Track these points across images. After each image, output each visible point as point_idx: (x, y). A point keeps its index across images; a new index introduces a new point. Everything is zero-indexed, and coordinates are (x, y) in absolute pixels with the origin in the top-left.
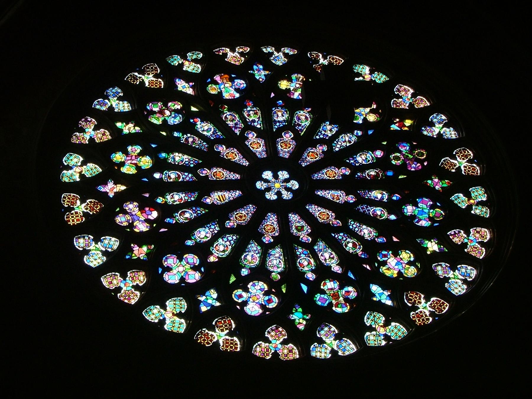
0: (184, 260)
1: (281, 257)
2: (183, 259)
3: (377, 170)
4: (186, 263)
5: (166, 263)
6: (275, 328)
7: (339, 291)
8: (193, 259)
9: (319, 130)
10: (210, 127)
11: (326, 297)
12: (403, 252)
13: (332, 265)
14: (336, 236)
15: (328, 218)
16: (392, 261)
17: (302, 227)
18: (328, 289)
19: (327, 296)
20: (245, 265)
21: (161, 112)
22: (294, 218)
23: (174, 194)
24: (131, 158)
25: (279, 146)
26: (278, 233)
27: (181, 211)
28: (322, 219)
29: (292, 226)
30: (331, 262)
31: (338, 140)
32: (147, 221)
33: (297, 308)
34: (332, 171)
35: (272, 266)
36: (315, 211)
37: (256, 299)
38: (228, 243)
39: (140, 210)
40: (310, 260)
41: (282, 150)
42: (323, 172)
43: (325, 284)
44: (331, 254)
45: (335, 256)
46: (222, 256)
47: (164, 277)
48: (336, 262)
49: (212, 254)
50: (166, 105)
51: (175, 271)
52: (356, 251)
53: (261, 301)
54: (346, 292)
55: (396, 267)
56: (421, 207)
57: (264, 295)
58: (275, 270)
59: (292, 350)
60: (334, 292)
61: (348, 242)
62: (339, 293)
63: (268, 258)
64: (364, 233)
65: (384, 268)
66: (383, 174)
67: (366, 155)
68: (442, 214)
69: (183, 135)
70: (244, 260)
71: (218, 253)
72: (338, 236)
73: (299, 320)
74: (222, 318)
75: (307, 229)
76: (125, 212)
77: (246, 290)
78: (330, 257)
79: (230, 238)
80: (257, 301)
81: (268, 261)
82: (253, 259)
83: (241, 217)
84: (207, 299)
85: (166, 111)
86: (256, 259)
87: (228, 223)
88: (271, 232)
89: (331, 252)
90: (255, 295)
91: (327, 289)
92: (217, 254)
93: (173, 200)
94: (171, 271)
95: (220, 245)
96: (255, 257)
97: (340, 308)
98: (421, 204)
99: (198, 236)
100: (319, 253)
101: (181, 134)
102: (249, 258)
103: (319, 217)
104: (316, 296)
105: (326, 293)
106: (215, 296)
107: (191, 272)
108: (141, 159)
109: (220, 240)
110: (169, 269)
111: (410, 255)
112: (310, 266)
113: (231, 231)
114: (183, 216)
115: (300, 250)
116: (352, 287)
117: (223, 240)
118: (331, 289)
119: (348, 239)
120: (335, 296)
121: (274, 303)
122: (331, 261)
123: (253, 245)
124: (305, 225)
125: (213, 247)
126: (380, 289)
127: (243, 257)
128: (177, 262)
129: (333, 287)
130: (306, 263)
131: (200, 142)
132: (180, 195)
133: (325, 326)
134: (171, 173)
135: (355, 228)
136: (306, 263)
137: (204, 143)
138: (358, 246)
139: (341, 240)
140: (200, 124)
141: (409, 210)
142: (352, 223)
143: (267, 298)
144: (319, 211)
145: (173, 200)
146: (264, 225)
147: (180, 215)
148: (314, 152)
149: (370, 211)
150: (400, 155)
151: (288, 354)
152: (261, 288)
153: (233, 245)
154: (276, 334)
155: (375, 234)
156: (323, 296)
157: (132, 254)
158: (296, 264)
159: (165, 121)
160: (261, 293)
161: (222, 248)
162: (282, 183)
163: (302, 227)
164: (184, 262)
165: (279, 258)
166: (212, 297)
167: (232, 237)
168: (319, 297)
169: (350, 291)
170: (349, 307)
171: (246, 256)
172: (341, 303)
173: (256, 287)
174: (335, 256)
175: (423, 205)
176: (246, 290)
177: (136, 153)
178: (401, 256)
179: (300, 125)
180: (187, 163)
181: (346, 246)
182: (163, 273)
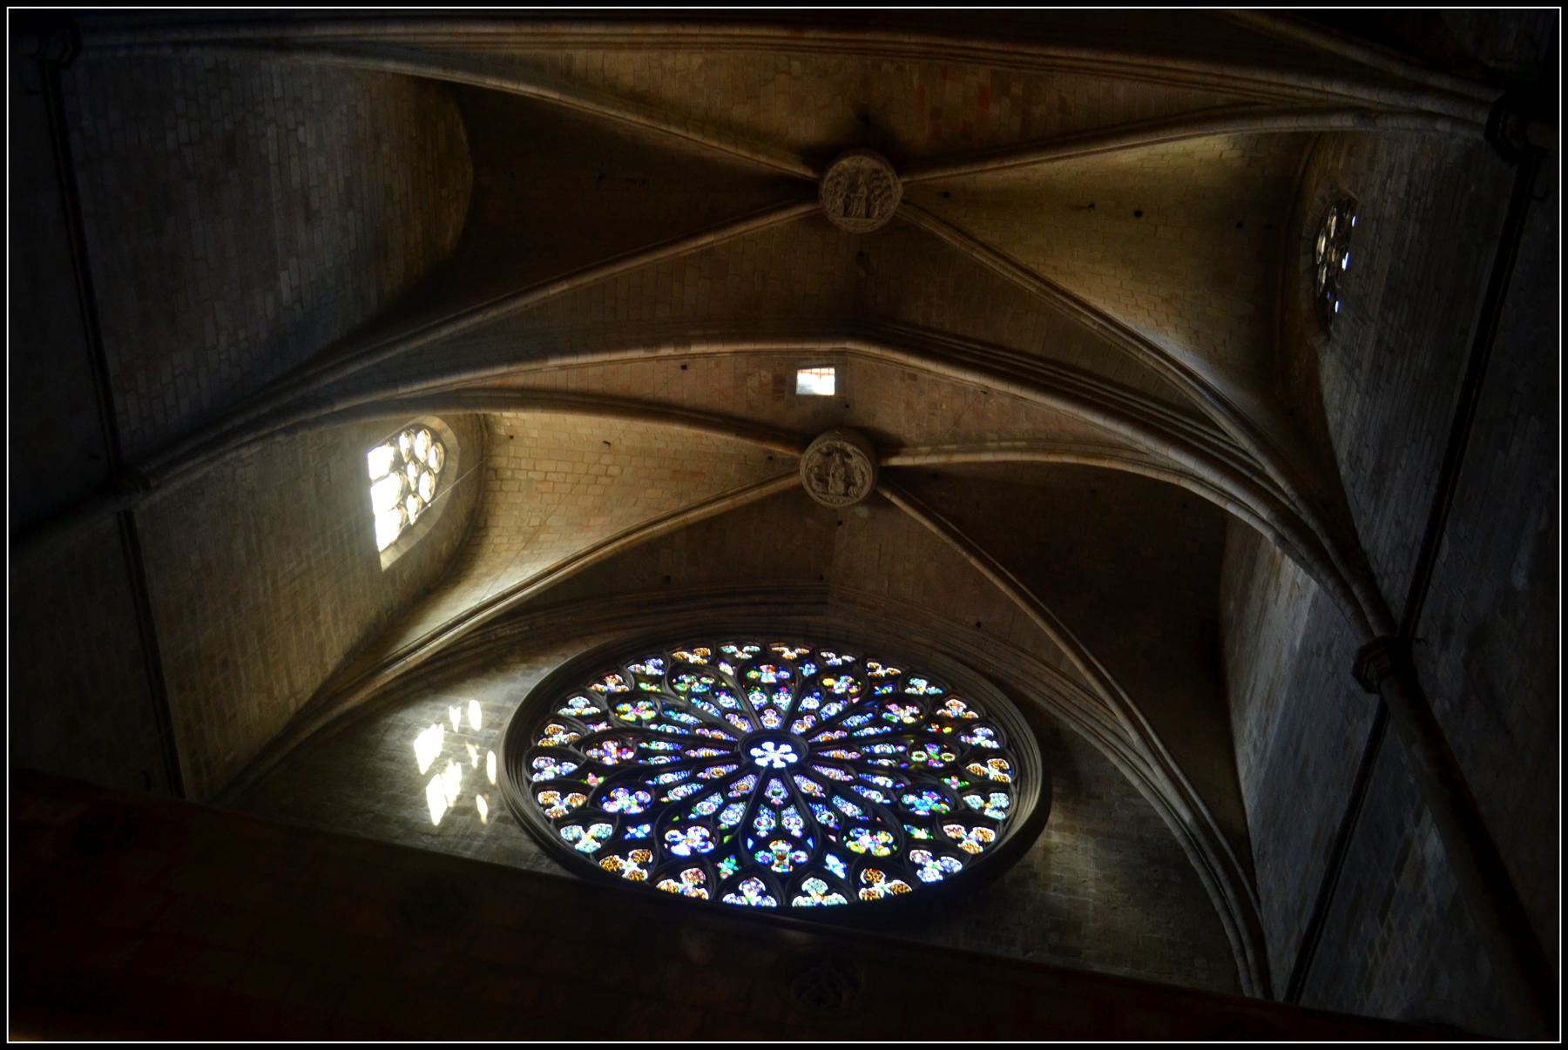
49: (667, 796)
53: (695, 845)
75: (784, 794)
110: (613, 800)
113: (701, 781)
136: (764, 822)
143: (703, 844)
156: (767, 854)
182: (606, 801)
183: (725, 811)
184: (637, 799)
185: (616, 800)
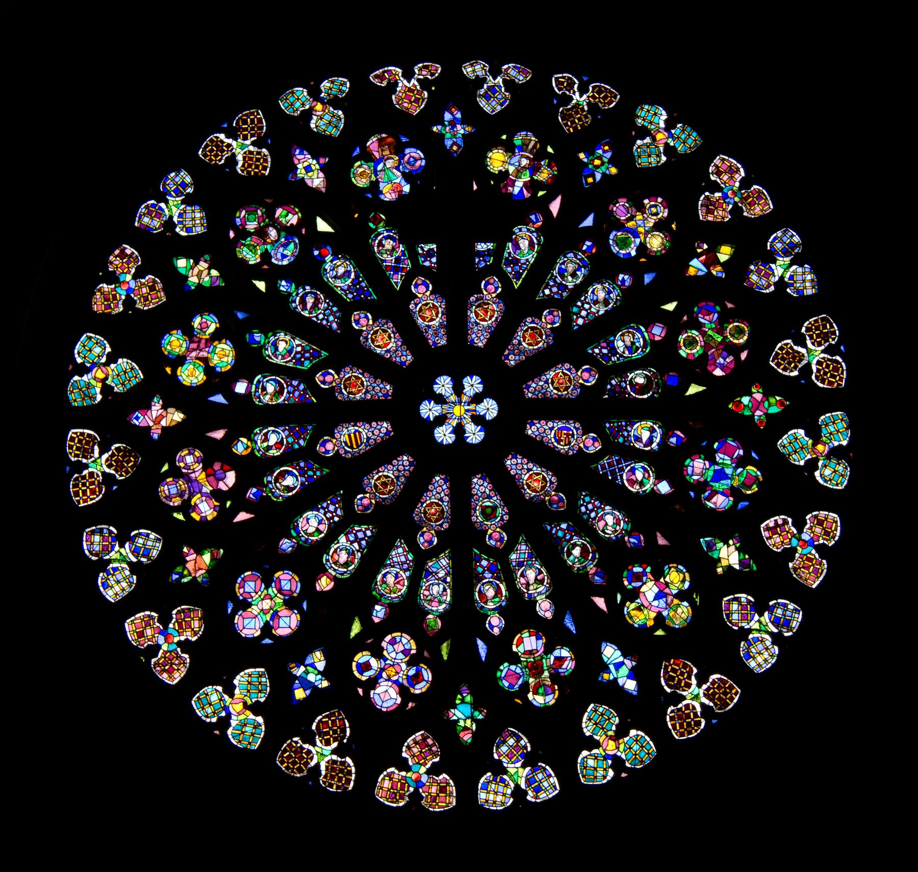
0: (273, 584)
1: (449, 579)
2: (273, 581)
3: (650, 371)
4: (276, 592)
5: (241, 591)
6: (420, 738)
7: (545, 656)
8: (288, 580)
9: (553, 274)
10: (349, 269)
11: (518, 671)
12: (673, 569)
13: (538, 598)
14: (554, 531)
15: (543, 488)
16: (649, 589)
17: (494, 508)
18: (526, 653)
19: (521, 669)
20: (381, 597)
21: (261, 233)
22: (480, 486)
23: (269, 431)
24: (199, 346)
25: (473, 315)
26: (448, 522)
27: (279, 471)
28: (532, 491)
29: (477, 505)
30: (539, 590)
31: (585, 299)
32: (216, 494)
33: (464, 695)
34: (565, 374)
35: (429, 598)
36: (521, 470)
37: (394, 674)
38: (356, 545)
39: (204, 469)
40: (501, 585)
41: (477, 324)
42: (548, 376)
43: (521, 641)
44: (540, 572)
45: (546, 577)
46: (342, 574)
47: (236, 622)
48: (547, 591)
49: (323, 571)
50: (270, 214)
51: (255, 610)
52: (585, 567)
54: (556, 658)
55: (656, 603)
56: (721, 461)
57: (409, 664)
58: (434, 609)
59: (446, 786)
60: (534, 658)
61: (575, 545)
62: (544, 661)
63: (425, 580)
64: (606, 524)
65: (633, 606)
66: (660, 381)
67: (633, 335)
68: (758, 479)
69: (297, 288)
70: (381, 586)
71: (336, 568)
72: (557, 531)
73: (465, 720)
74: (331, 714)
76: (176, 473)
77: (378, 653)
78: (536, 579)
79: (360, 535)
80: (394, 678)
81: (424, 588)
82: (398, 583)
83: (385, 484)
84: (307, 672)
85: (271, 228)
86: (401, 583)
87: (361, 499)
88: (436, 521)
89: (539, 567)
90: (392, 663)
91: (522, 651)
92: (335, 570)
93: (265, 444)
94: (250, 610)
95: (341, 550)
96: (401, 578)
97: (542, 695)
98: (722, 456)
99: (304, 529)
100: (519, 570)
101: (293, 286)
102: (390, 579)
103: (527, 484)
104: (502, 668)
105: (520, 662)
106: (321, 666)
107: (284, 612)
108: (215, 347)
109: (342, 539)
110: (245, 605)
111: (684, 577)
112: (497, 599)
114: (280, 483)
115: (484, 563)
116: (568, 649)
117: (348, 540)
118: (530, 653)
119: (575, 537)
120: (536, 668)
121: (424, 683)
122: (537, 589)
123: (400, 550)
124: (500, 505)
125: (328, 554)
126: (618, 653)
127: (379, 577)
128: (262, 590)
129: (534, 648)
130: (491, 593)
131: (326, 305)
132: (279, 433)
133: (510, 735)
134: (267, 381)
135: (592, 511)
136: (491, 593)
137: (335, 309)
138: (591, 555)
139: (561, 538)
140: (331, 261)
141: (697, 467)
142: (587, 499)
144: (529, 470)
145: (265, 444)
146: (425, 505)
147: (276, 481)
148: (536, 328)
149: (624, 471)
150: (697, 333)
151: (438, 795)
152: (405, 649)
153: (364, 549)
154: (421, 752)
155: (625, 528)
156: (513, 667)
157: (183, 570)
158: (473, 595)
159: (266, 256)
160: (404, 660)
161: (343, 557)
162: (469, 405)
163: (494, 508)
164: (272, 591)
165: (444, 581)
166: (315, 668)
167: (365, 533)
168: (506, 669)
169: (564, 657)
170: (557, 692)
171: (385, 575)
172: (544, 685)
173: (396, 646)
174: (546, 577)
175: (726, 457)
176: (378, 653)
177: (207, 333)
178: (667, 579)
179: (516, 261)
180: (298, 356)
181: (569, 554)
182: (234, 612)
183: (424, 584)
184: (280, 590)
185: (250, 605)
